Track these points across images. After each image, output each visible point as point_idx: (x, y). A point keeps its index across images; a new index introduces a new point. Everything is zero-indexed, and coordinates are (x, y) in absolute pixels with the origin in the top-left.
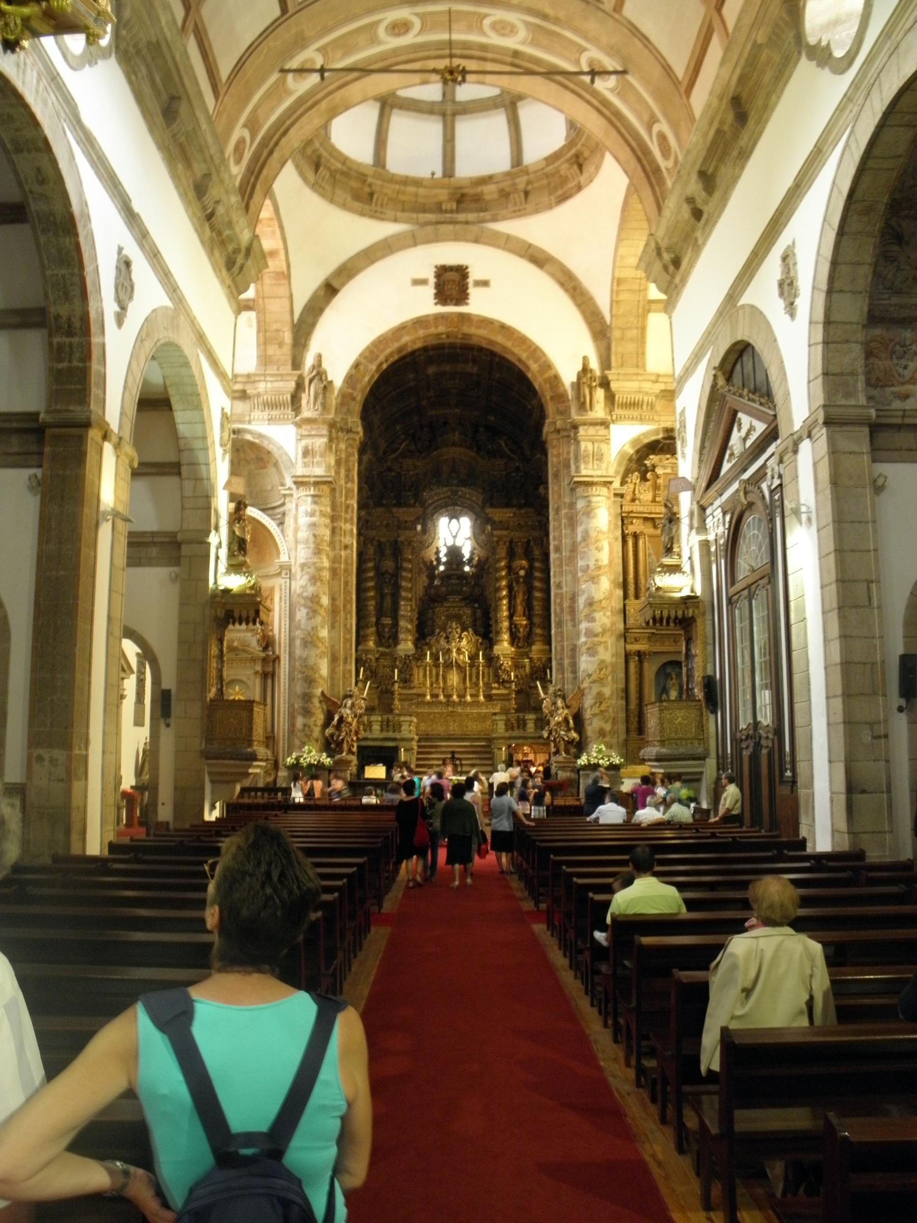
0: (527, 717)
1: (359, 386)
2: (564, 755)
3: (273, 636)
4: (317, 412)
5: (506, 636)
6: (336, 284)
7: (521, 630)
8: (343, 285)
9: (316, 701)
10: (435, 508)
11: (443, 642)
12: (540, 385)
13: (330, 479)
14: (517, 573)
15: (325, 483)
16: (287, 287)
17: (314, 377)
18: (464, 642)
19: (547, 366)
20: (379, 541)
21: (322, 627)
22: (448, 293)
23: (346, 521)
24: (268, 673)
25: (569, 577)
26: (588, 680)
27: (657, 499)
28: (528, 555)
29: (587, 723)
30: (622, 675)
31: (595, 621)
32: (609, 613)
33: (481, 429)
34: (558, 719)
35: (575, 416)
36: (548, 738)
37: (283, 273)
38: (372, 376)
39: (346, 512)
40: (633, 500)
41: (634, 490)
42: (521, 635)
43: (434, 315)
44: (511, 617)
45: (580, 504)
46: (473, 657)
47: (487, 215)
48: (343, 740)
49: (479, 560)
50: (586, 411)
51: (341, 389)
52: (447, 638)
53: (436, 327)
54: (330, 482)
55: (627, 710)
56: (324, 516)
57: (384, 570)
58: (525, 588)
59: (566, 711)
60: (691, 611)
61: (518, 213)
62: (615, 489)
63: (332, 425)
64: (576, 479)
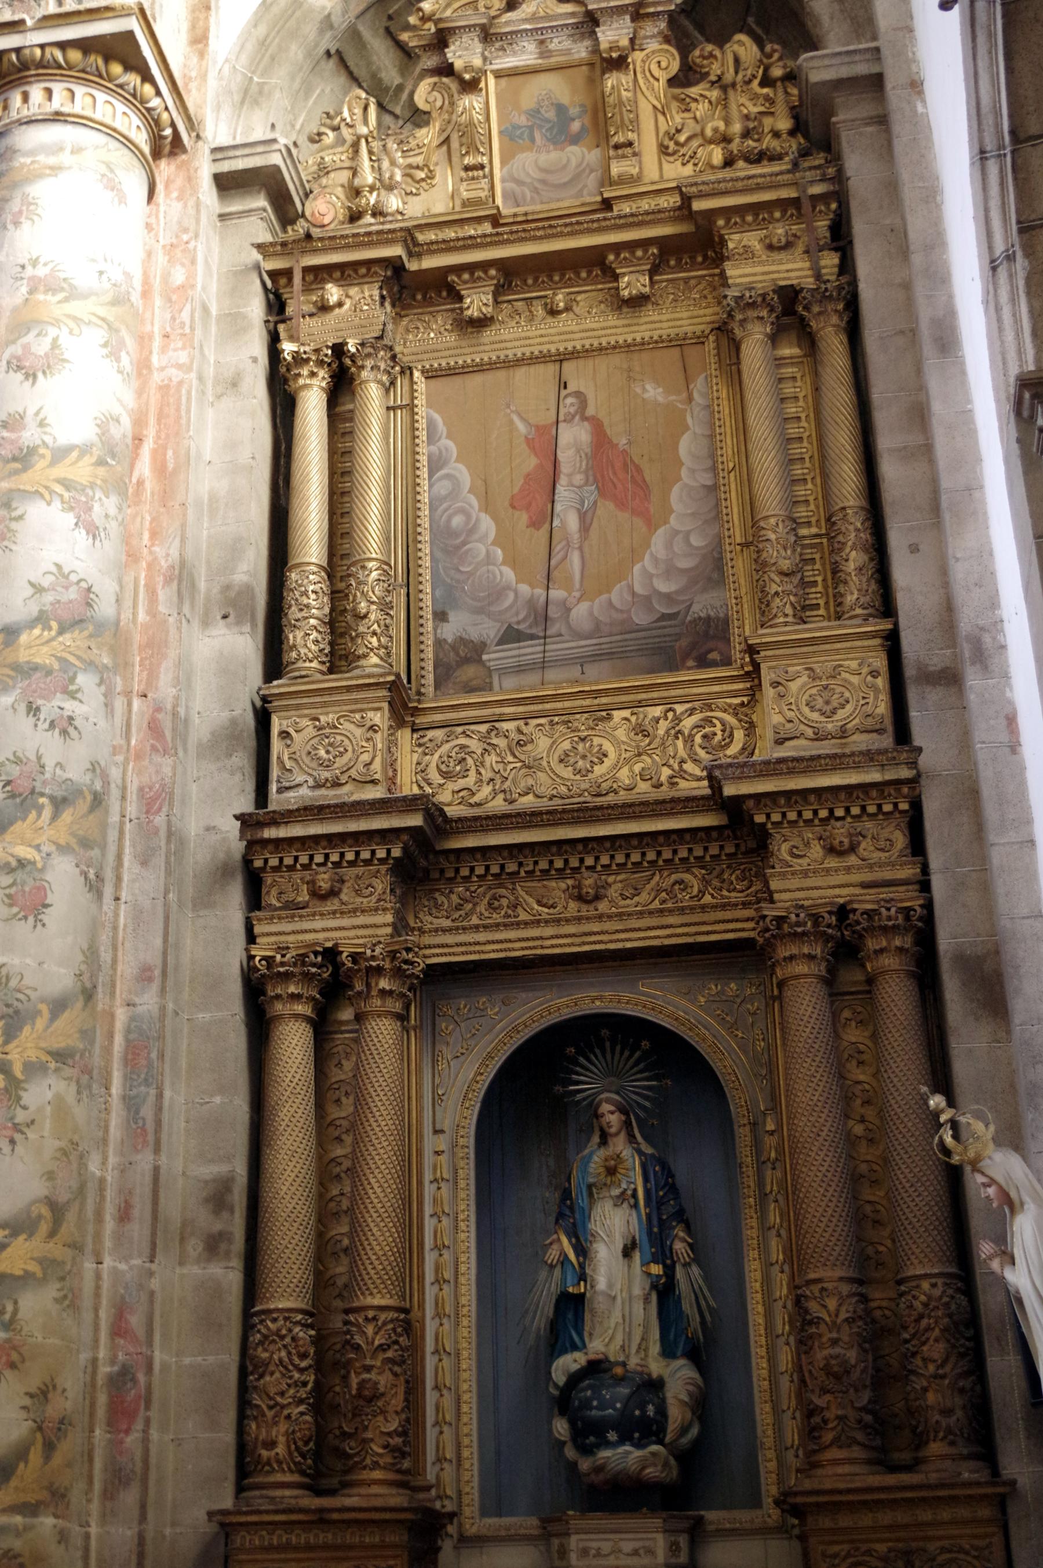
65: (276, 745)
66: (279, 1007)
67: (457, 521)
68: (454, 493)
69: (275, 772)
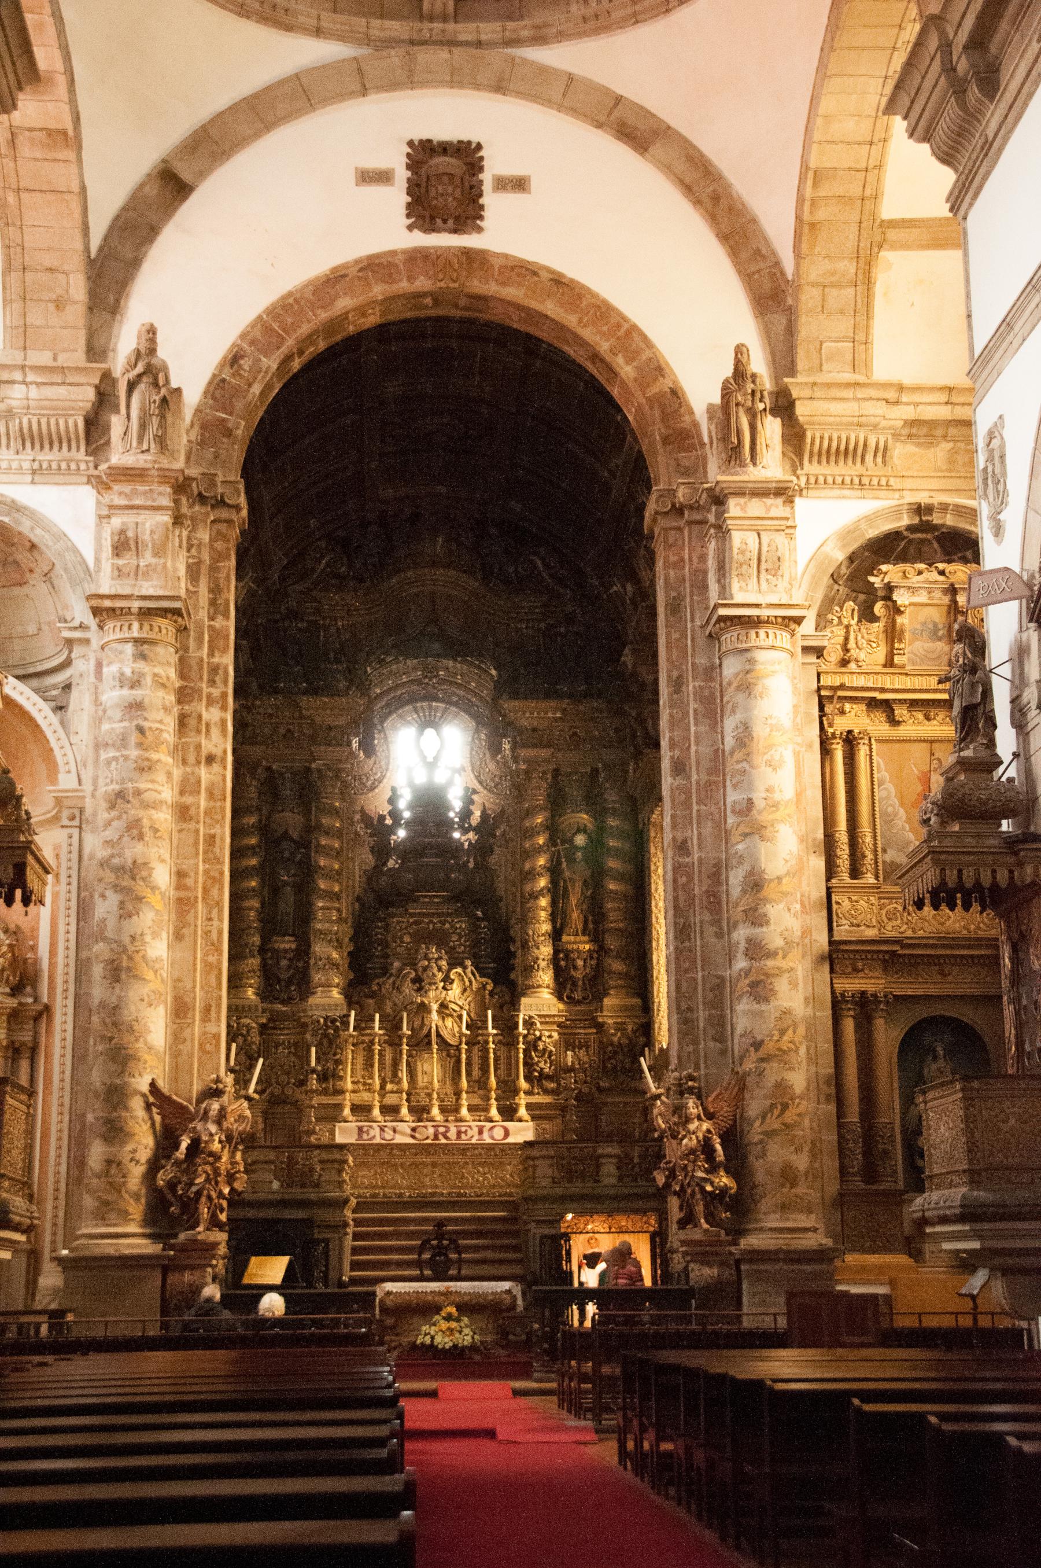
0: (600, 1151)
1: (239, 405)
2: (706, 1226)
3: (36, 962)
4: (148, 457)
5: (545, 977)
6: (186, 176)
7: (580, 963)
8: (202, 175)
9: (137, 1105)
10: (388, 705)
11: (408, 989)
12: (639, 410)
13: (177, 605)
14: (571, 841)
15: (164, 612)
16: (74, 168)
17: (140, 376)
18: (456, 990)
19: (658, 369)
20: (268, 769)
21: (155, 935)
22: (439, 203)
23: (210, 702)
24: (23, 1044)
25: (708, 828)
26: (753, 1055)
27: (897, 659)
28: (593, 801)
29: (756, 1150)
30: (826, 1046)
31: (768, 923)
32: (798, 907)
34: (689, 1143)
35: (715, 474)
36: (667, 1186)
37: (64, 133)
38: (268, 387)
39: (212, 682)
40: (844, 663)
41: (846, 639)
42: (578, 975)
43: (404, 252)
44: (556, 935)
45: (731, 668)
46: (476, 1026)
47: (523, 28)
48: (199, 1194)
49: (484, 816)
50: (743, 465)
51: (198, 411)
52: (418, 980)
53: (411, 279)
54: (177, 612)
55: (840, 1126)
56: (164, 686)
57: (281, 831)
58: (588, 873)
59: (705, 1126)
60: (1029, 870)
61: (592, 24)
62: (804, 637)
63: (181, 486)
64: (722, 612)
65: (835, 907)
66: (845, 1013)
67: (890, 809)
68: (888, 797)
69: (835, 917)
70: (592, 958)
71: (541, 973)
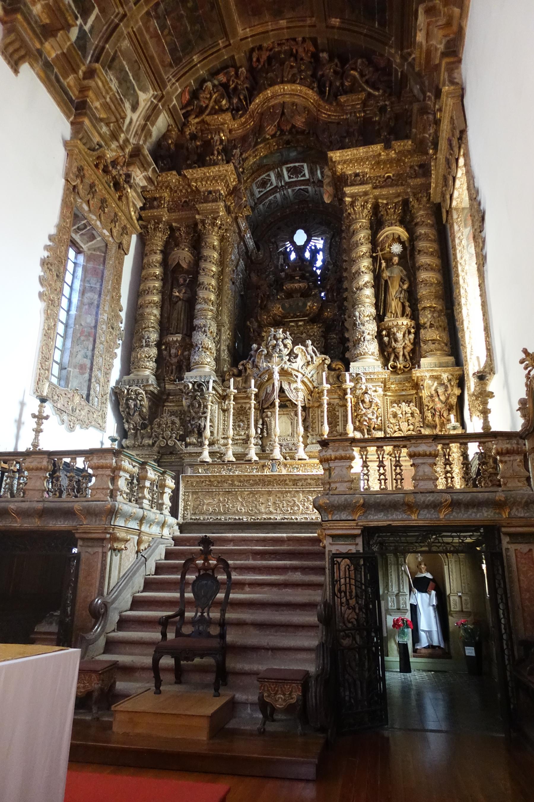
7: (400, 335)
33: (324, 55)
44: (379, 318)
70: (410, 333)
71: (366, 343)
